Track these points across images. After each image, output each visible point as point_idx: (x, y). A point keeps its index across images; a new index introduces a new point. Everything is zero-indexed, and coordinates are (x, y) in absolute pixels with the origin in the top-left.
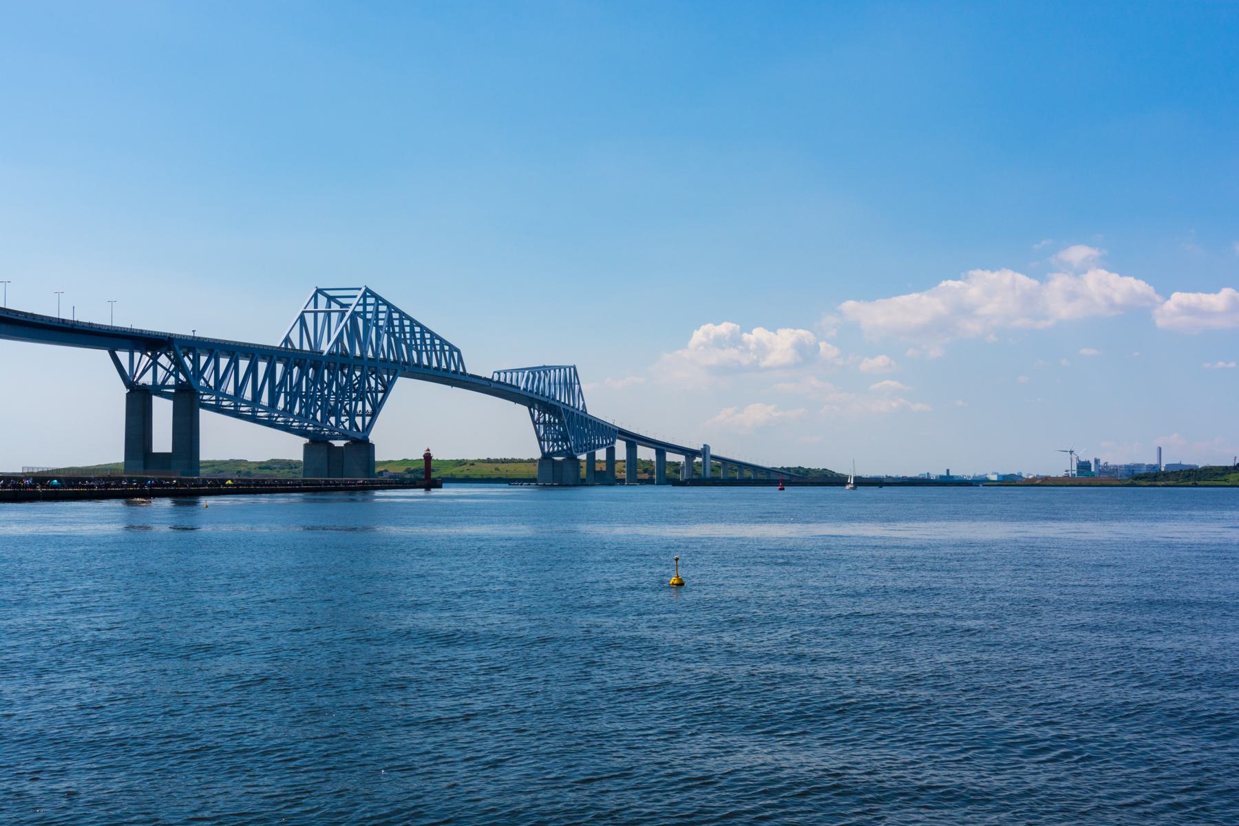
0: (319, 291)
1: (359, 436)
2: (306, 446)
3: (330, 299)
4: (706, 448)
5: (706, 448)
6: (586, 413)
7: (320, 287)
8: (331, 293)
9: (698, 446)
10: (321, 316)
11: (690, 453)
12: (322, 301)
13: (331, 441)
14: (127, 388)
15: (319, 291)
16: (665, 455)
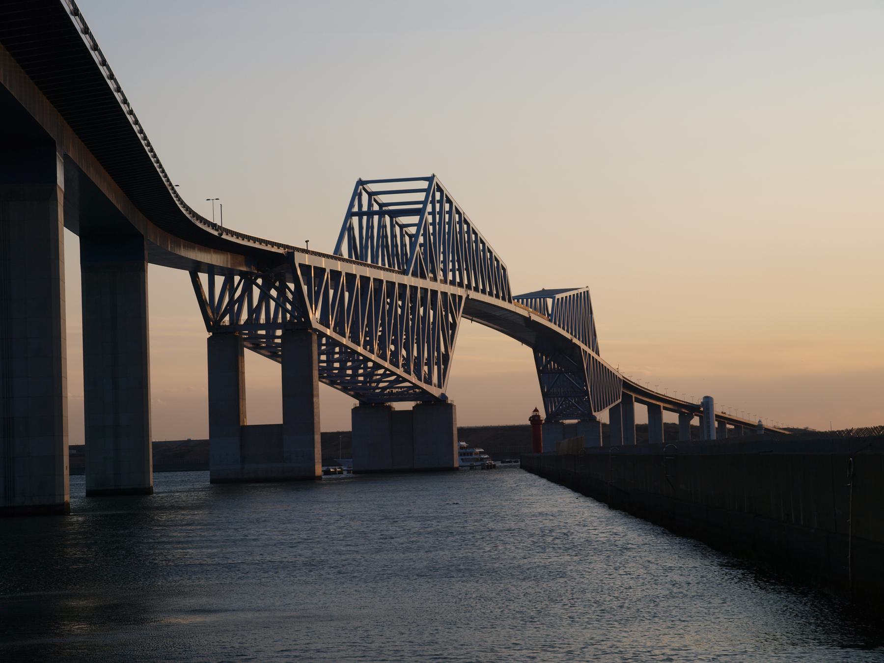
0: (361, 183)
1: (435, 392)
2: (355, 411)
3: (371, 194)
4: (708, 401)
5: (708, 401)
6: (598, 353)
7: (364, 179)
8: (372, 187)
9: (697, 401)
10: (365, 218)
11: (685, 409)
12: (365, 197)
13: (389, 403)
14: (209, 331)
15: (361, 183)
16: (660, 413)
